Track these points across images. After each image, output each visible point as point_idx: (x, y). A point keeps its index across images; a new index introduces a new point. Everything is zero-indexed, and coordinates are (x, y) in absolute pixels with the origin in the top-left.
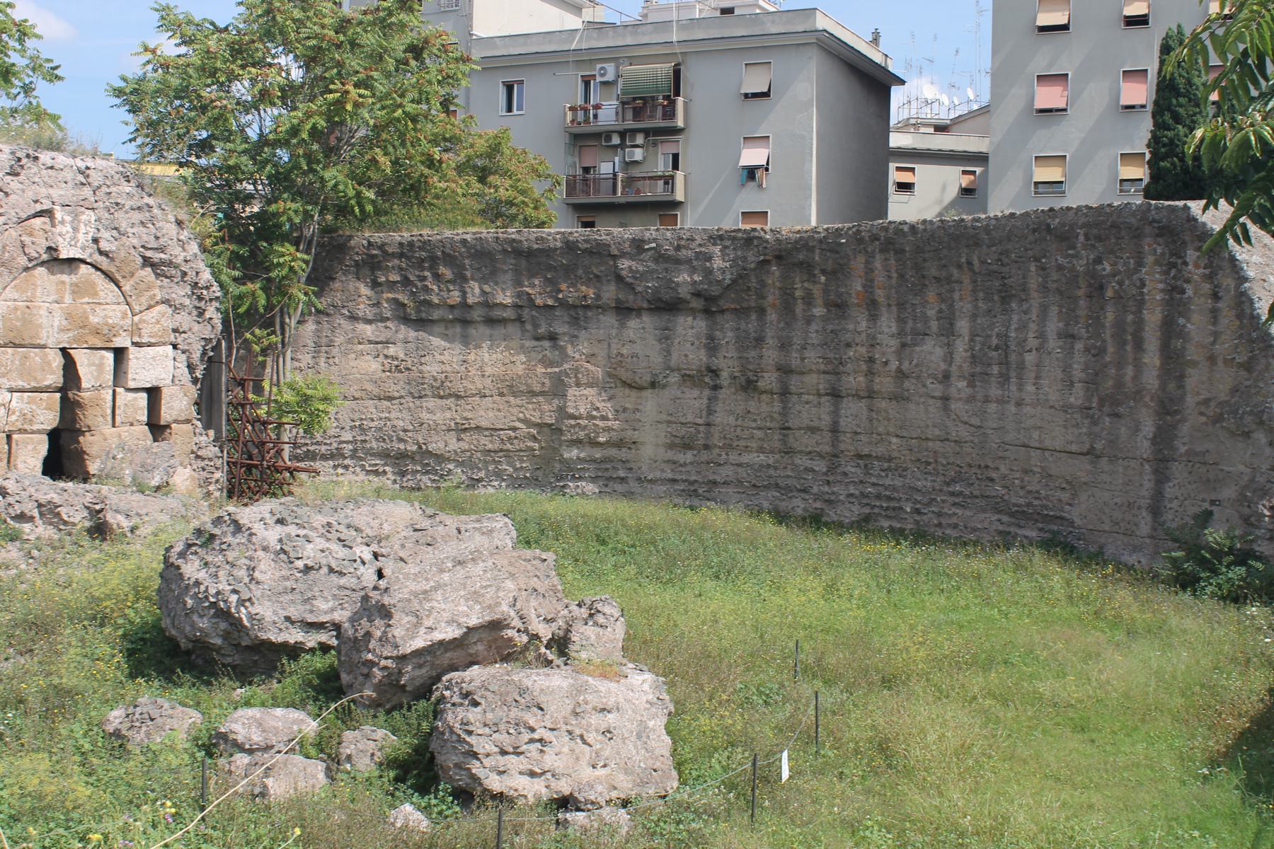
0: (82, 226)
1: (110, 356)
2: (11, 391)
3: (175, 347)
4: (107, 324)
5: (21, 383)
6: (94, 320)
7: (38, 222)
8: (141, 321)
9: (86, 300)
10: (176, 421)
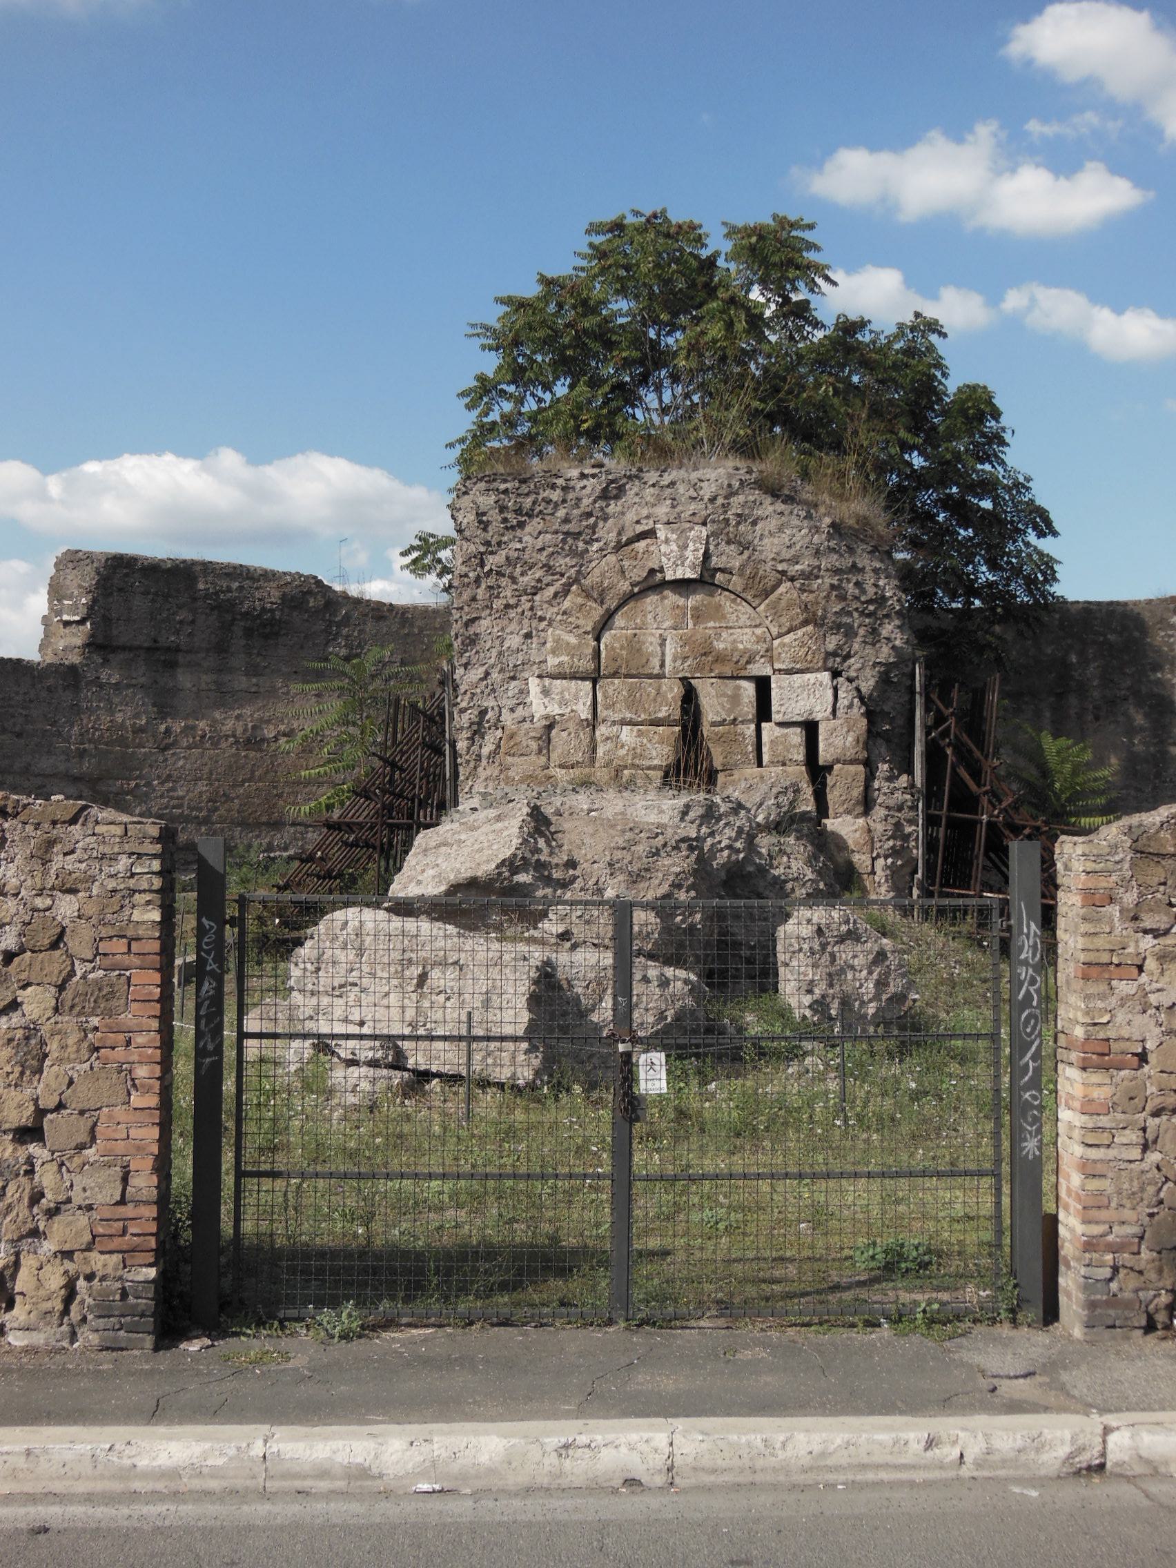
0: (691, 544)
1: (749, 689)
2: (623, 723)
3: (836, 674)
4: (735, 649)
5: (628, 715)
6: (720, 646)
7: (642, 545)
8: (784, 645)
9: (711, 624)
10: (838, 761)
